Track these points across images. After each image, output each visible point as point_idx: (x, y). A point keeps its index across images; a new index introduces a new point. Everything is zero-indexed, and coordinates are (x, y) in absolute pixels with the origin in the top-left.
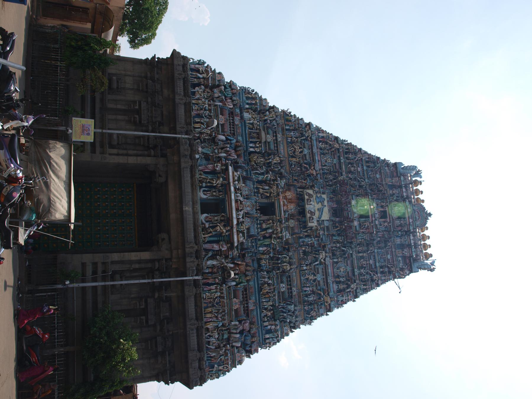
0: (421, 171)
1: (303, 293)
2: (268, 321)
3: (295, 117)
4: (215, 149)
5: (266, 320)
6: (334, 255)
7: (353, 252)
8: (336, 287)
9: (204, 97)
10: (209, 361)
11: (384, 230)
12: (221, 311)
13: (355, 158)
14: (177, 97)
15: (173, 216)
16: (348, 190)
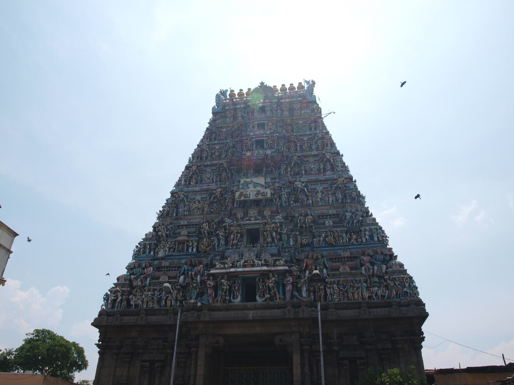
0: (221, 90)
2: (361, 238)
3: (165, 207)
4: (193, 286)
5: (360, 240)
6: (298, 174)
7: (296, 156)
9: (141, 295)
10: (401, 296)
11: (276, 125)
12: (352, 284)
13: (207, 151)
15: (258, 330)
16: (236, 158)
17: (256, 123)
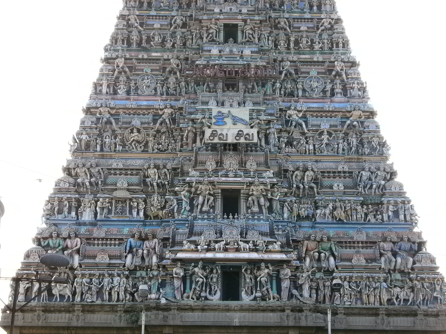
2: (382, 214)
3: (82, 134)
5: (380, 216)
6: (291, 94)
7: (288, 60)
8: (339, 98)
10: (429, 302)
12: (368, 283)
14: (74, 323)
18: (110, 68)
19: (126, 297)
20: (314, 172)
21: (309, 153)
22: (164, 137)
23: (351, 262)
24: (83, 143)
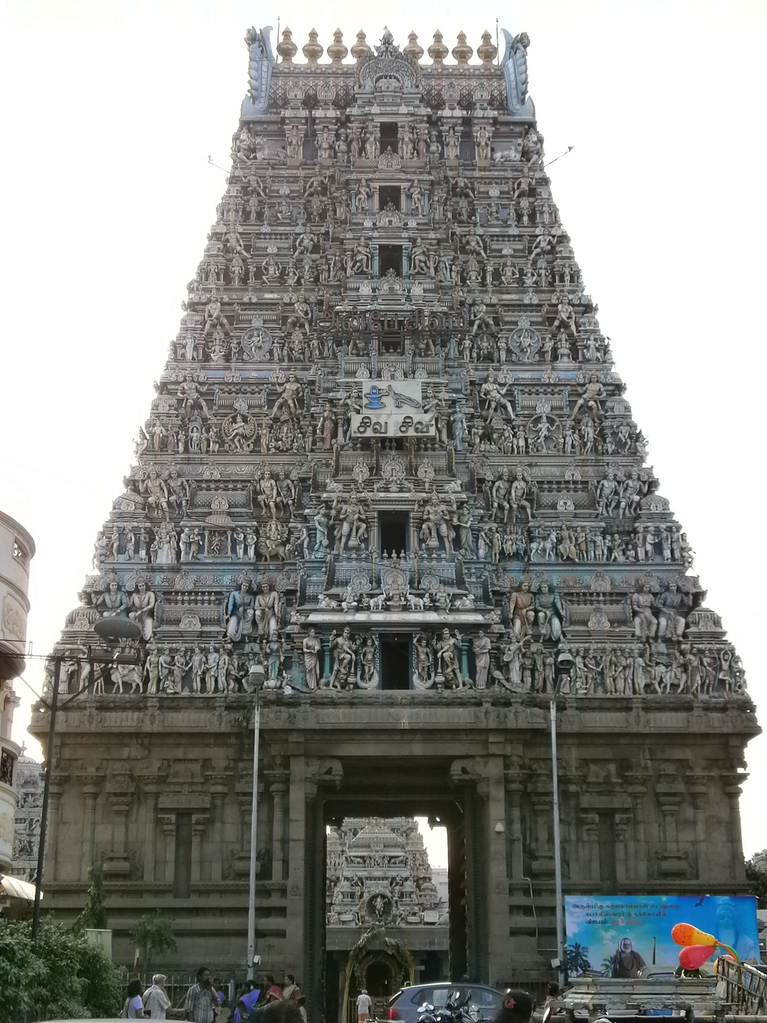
1: (578, 453)
2: (635, 548)
3: (154, 425)
6: (489, 358)
7: (482, 303)
8: (565, 363)
10: (711, 689)
12: (614, 659)
14: (147, 728)
15: (418, 749)
17: (377, 185)
18: (198, 318)
19: (228, 685)
20: (527, 482)
21: (519, 453)
22: (285, 429)
23: (587, 625)
24: (156, 440)
